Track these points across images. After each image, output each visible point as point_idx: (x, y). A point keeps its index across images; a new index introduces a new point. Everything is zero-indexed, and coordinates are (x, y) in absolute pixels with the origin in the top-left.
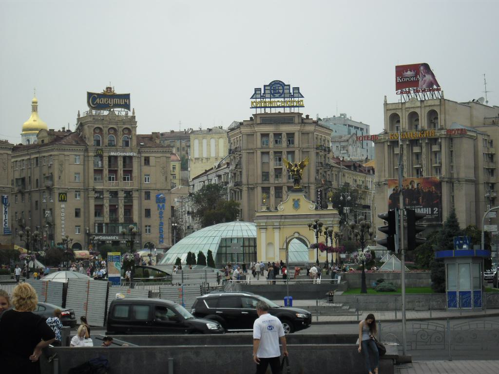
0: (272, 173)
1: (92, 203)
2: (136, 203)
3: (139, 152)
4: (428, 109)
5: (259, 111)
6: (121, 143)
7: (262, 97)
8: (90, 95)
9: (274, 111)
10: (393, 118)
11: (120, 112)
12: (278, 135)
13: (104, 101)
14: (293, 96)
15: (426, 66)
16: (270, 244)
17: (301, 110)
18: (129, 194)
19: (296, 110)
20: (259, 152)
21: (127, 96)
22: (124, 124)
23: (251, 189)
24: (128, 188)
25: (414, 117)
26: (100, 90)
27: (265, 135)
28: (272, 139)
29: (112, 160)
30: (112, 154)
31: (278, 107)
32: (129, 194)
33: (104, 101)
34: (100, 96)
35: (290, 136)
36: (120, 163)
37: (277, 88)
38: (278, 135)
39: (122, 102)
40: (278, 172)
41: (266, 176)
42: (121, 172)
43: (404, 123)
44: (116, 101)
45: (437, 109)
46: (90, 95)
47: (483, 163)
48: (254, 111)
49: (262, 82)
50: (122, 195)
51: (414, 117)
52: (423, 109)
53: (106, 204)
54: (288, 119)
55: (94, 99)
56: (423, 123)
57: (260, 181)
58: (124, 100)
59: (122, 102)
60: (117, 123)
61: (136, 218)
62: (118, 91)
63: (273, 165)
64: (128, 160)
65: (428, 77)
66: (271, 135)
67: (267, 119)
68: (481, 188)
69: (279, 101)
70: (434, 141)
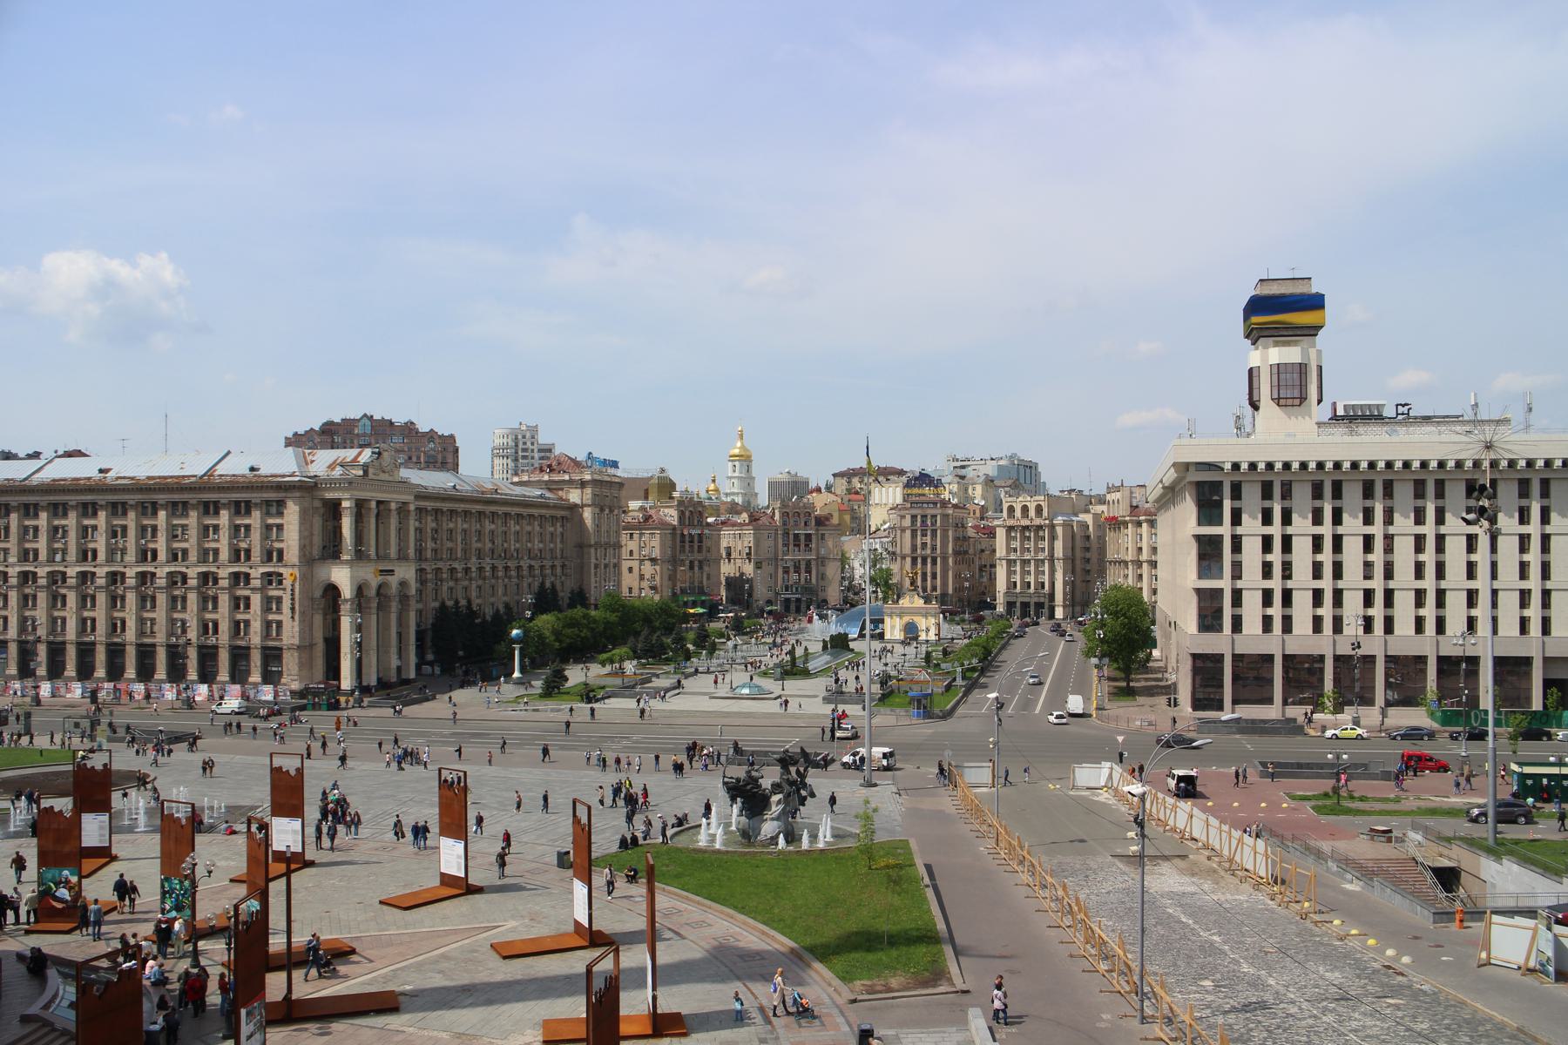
1: (780, 571)
16: (893, 627)
18: (808, 563)
23: (903, 558)
25: (1025, 509)
29: (796, 536)
32: (808, 563)
35: (934, 516)
40: (924, 545)
43: (1018, 513)
47: (1079, 543)
51: (1025, 509)
61: (814, 581)
64: (808, 537)
68: (1078, 562)
70: (1040, 527)
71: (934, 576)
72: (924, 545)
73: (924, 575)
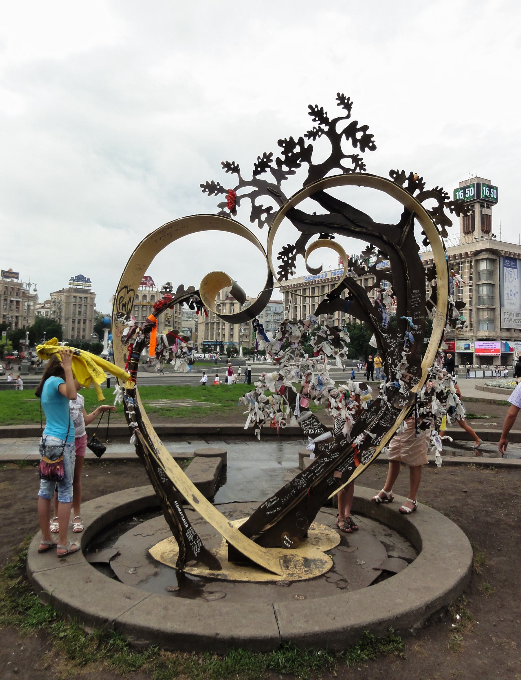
0: (77, 313)
2: (20, 322)
3: (23, 299)
4: (151, 294)
5: (72, 286)
6: (15, 294)
7: (73, 281)
8: (2, 271)
9: (78, 287)
11: (15, 280)
12: (80, 298)
13: (7, 274)
14: (86, 282)
15: (150, 278)
17: (90, 288)
19: (88, 288)
20: (72, 304)
21: (18, 274)
22: (17, 286)
23: (67, 319)
24: (17, 315)
26: (7, 270)
27: (75, 297)
30: (12, 299)
31: (80, 285)
32: (17, 317)
34: (7, 272)
35: (86, 298)
36: (15, 303)
37: (80, 278)
39: (16, 276)
40: (80, 313)
41: (74, 314)
44: (13, 275)
45: (155, 295)
46: (2, 271)
48: (70, 286)
49: (75, 274)
54: (86, 291)
55: (4, 273)
56: (149, 299)
57: (71, 316)
59: (16, 276)
60: (14, 285)
62: (14, 271)
63: (78, 310)
64: (18, 302)
65: (151, 282)
66: (78, 297)
67: (77, 291)
69: (81, 283)
71: (84, 330)
72: (80, 313)
73: (78, 329)
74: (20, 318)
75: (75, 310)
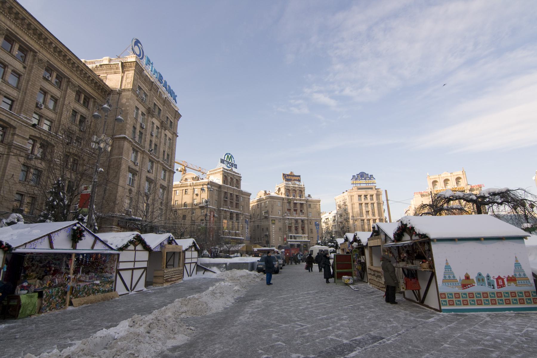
8: (284, 174)
10: (435, 183)
11: (297, 182)
13: (289, 178)
21: (299, 176)
26: (289, 173)
27: (360, 196)
28: (363, 197)
33: (289, 178)
34: (288, 175)
36: (298, 206)
37: (362, 175)
38: (366, 196)
39: (297, 178)
42: (299, 211)
46: (284, 174)
50: (300, 221)
52: (452, 177)
53: (293, 226)
58: (298, 178)
59: (297, 178)
62: (295, 174)
69: (364, 181)
74: (306, 222)
75: (361, 209)
